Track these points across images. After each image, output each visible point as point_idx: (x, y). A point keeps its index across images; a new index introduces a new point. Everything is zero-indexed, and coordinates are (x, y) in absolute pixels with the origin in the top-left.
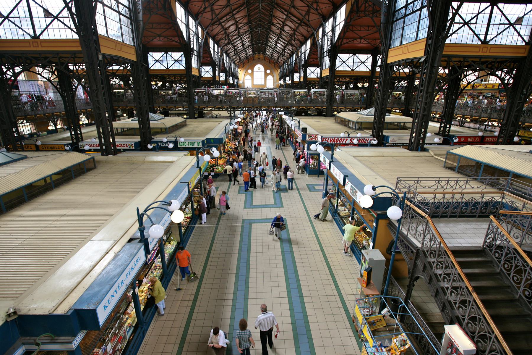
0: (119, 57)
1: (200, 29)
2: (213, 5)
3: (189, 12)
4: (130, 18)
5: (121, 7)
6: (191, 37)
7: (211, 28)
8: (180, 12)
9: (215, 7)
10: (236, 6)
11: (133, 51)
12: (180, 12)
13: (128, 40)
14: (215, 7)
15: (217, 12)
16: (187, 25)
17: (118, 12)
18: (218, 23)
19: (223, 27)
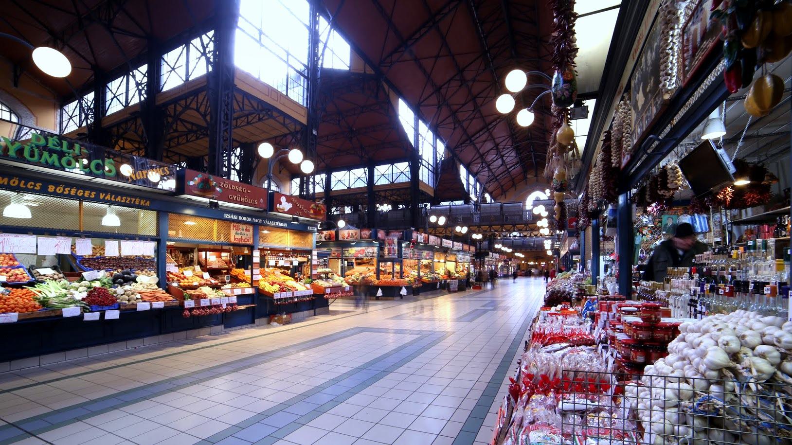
0: (426, 193)
1: (478, 185)
2: (490, 165)
3: (470, 172)
4: (433, 172)
5: (430, 166)
6: (471, 189)
7: (488, 185)
8: (463, 171)
9: (491, 167)
10: (510, 166)
11: (433, 191)
12: (463, 171)
13: (431, 185)
14: (491, 167)
15: (494, 171)
16: (468, 180)
17: (428, 168)
18: (494, 180)
19: (499, 183)
